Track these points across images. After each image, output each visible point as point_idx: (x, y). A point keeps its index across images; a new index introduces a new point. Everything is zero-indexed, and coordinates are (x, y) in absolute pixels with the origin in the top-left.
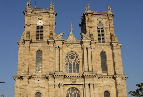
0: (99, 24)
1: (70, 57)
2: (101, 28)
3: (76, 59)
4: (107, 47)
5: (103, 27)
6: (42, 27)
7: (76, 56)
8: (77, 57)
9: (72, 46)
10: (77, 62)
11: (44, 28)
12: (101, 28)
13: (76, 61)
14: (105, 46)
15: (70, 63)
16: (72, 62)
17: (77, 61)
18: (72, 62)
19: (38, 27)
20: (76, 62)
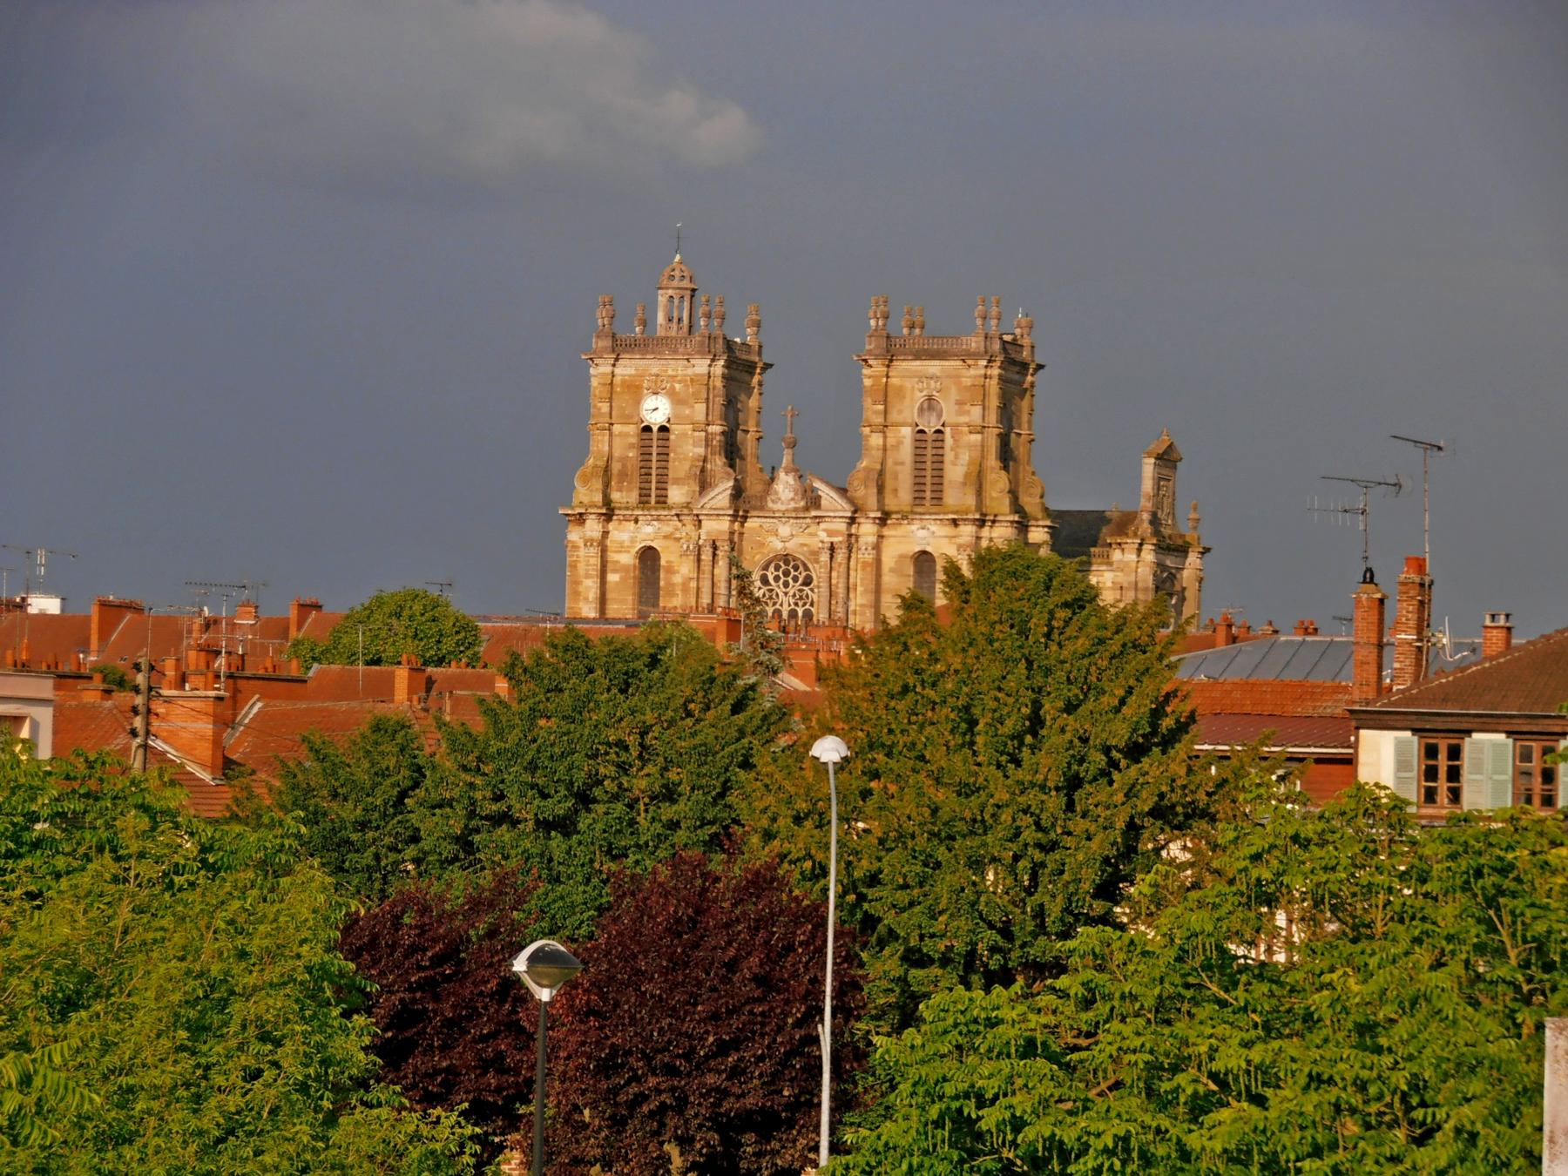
0: (925, 406)
1: (777, 579)
2: (930, 425)
3: (801, 591)
4: (943, 534)
5: (943, 425)
6: (663, 429)
7: (804, 574)
8: (808, 582)
9: (785, 530)
10: (805, 604)
11: (672, 437)
12: (930, 425)
13: (801, 598)
14: (933, 528)
15: (777, 606)
16: (785, 606)
17: (807, 596)
18: (785, 606)
19: (647, 429)
20: (800, 603)
